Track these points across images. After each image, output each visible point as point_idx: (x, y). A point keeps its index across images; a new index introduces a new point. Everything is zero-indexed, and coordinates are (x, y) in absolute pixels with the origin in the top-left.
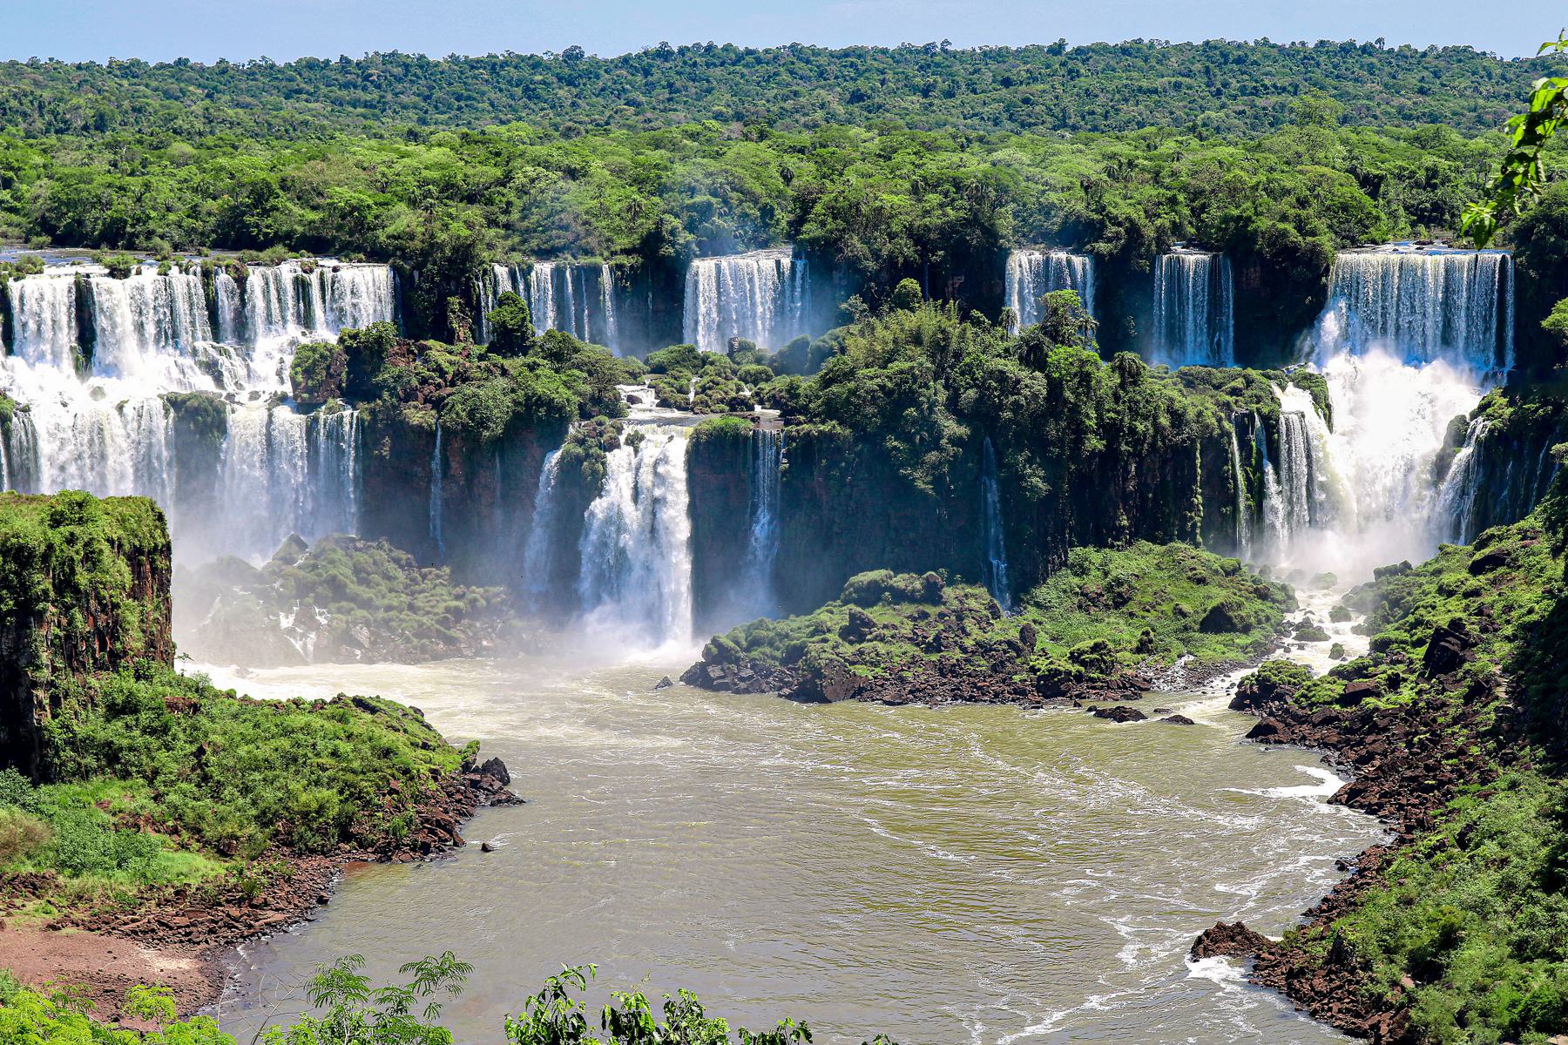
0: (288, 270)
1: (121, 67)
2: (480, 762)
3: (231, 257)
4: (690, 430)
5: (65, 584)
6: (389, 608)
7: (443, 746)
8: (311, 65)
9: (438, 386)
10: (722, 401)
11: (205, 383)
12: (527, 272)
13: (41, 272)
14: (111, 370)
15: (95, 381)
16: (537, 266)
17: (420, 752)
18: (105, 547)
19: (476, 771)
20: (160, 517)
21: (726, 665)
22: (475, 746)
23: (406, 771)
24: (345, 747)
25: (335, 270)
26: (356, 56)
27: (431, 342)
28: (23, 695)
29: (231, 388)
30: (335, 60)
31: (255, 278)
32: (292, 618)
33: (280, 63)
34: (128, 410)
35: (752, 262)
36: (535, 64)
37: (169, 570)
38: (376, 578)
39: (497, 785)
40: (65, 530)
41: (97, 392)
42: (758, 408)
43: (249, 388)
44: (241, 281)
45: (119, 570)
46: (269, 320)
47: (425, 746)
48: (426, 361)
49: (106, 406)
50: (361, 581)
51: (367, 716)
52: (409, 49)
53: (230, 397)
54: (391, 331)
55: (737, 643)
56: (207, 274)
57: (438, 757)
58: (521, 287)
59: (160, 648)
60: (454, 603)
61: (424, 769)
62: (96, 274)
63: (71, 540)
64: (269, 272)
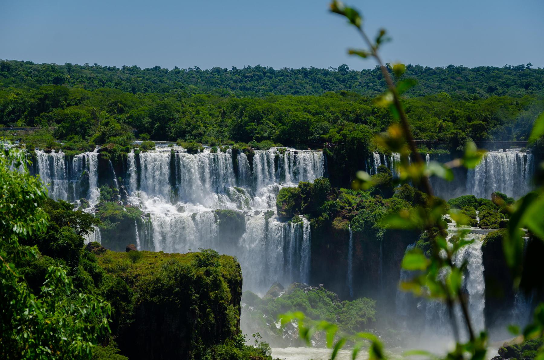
0: (272, 152)
1: (129, 69)
3: (246, 146)
5: (205, 296)
8: (218, 71)
9: (350, 211)
10: (495, 223)
11: (231, 206)
12: (388, 156)
13: (154, 149)
14: (188, 199)
15: (180, 203)
16: (393, 154)
20: (238, 266)
25: (296, 153)
26: (240, 68)
29: (245, 209)
30: (230, 69)
33: (203, 69)
34: (198, 217)
35: (504, 154)
36: (326, 73)
38: (320, 304)
40: (204, 269)
41: (181, 209)
43: (253, 210)
44: (250, 157)
46: (264, 177)
48: (341, 199)
49: (186, 215)
50: (313, 307)
52: (265, 64)
53: (245, 213)
54: (327, 182)
56: (235, 153)
58: (386, 164)
60: (360, 319)
62: (181, 151)
63: (208, 273)
64: (264, 152)
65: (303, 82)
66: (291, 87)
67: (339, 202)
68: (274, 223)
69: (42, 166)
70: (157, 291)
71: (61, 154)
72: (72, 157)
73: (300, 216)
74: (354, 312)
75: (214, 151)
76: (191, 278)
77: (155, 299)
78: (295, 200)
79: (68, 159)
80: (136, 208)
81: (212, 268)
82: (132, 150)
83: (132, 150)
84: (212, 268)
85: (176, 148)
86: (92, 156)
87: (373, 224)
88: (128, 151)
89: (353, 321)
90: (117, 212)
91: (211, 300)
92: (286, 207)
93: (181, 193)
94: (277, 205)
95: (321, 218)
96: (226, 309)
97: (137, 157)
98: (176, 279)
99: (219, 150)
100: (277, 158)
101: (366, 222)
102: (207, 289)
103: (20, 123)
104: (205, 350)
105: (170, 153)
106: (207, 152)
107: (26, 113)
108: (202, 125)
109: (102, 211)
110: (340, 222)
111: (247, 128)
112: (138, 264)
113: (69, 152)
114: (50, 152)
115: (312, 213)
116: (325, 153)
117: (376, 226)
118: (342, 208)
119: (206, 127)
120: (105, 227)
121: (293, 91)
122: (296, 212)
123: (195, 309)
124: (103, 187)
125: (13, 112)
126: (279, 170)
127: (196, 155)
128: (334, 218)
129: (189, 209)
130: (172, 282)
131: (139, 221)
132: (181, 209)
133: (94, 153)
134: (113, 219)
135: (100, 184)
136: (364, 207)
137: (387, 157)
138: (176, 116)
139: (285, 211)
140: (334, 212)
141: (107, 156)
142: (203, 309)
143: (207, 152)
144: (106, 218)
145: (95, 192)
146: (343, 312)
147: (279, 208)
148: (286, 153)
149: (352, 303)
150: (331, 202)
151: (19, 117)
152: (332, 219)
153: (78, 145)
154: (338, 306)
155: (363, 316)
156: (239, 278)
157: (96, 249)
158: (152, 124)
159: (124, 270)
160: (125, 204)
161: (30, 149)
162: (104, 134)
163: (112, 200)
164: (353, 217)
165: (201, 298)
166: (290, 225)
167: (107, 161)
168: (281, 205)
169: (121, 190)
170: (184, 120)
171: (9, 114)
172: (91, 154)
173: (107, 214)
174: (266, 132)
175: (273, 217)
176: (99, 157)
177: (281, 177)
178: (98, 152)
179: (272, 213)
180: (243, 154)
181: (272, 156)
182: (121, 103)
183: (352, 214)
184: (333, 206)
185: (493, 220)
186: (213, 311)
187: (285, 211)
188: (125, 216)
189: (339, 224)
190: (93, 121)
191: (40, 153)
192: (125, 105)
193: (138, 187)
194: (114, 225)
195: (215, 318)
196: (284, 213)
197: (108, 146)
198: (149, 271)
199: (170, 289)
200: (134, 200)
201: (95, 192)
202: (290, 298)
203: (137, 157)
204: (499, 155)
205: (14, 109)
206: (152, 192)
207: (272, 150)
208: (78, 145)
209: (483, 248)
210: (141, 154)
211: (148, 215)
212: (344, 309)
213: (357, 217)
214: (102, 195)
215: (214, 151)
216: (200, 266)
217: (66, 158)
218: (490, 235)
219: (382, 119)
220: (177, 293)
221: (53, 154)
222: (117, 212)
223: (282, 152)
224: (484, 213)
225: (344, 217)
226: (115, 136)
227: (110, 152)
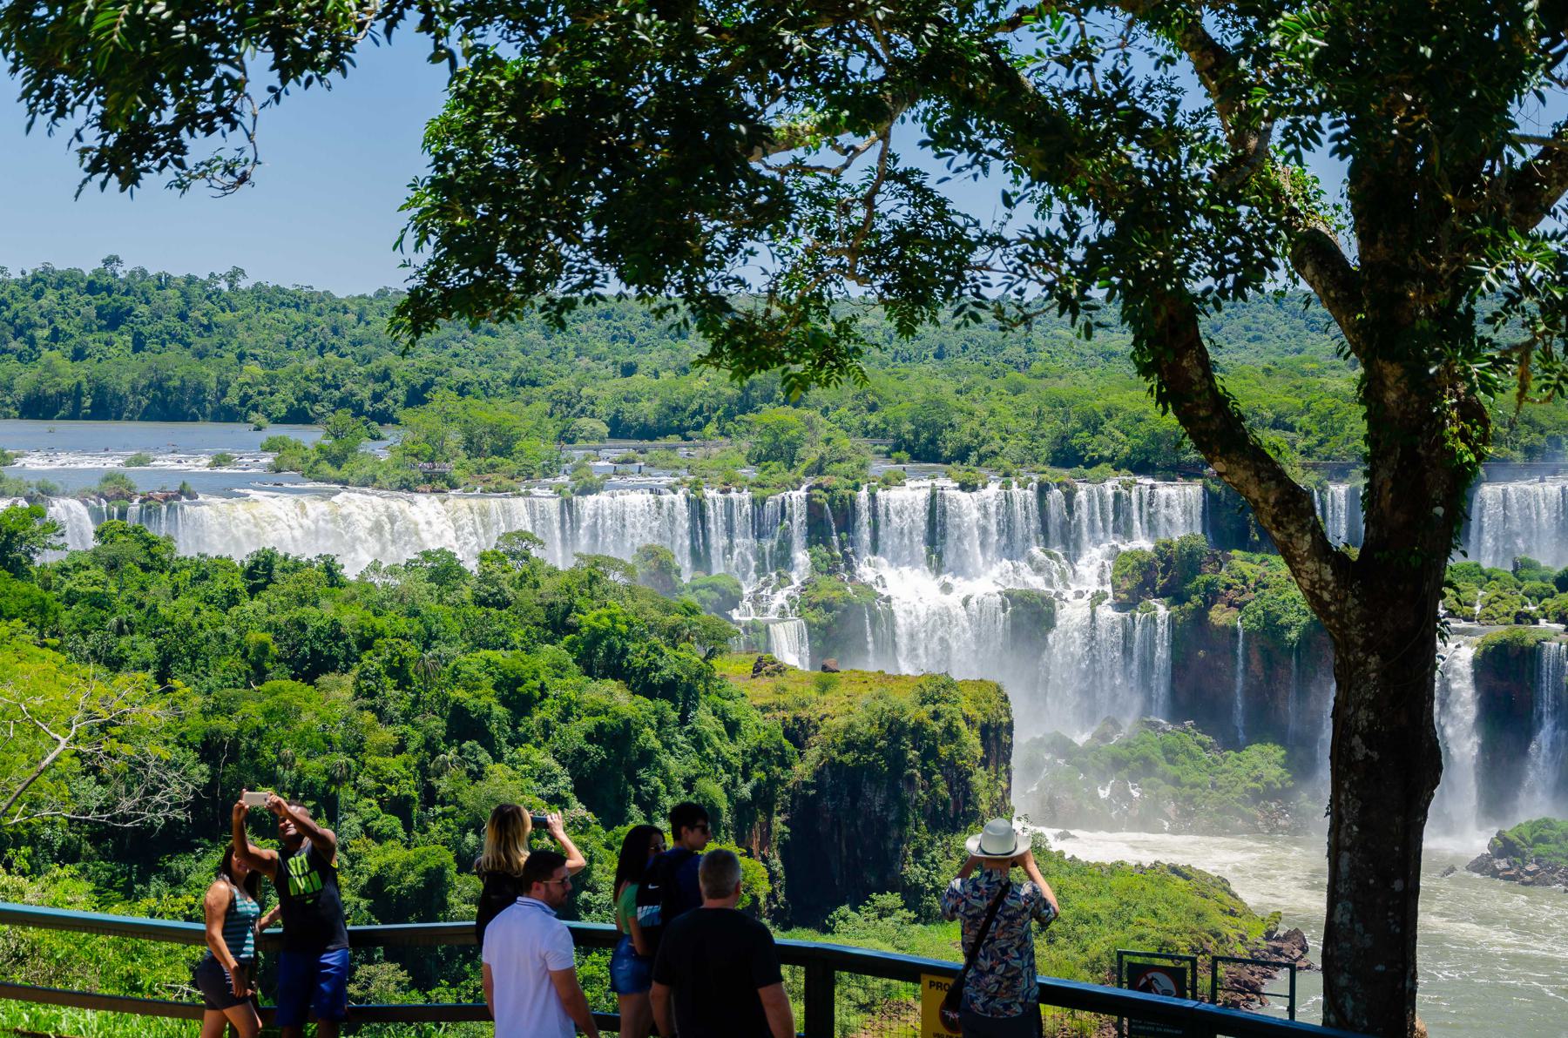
2: (1281, 933)
3: (1064, 474)
4: (1478, 640)
5: (930, 753)
6: (1194, 786)
7: (1247, 913)
9: (1243, 592)
10: (1507, 614)
11: (1037, 583)
14: (960, 571)
15: (948, 578)
16: (1332, 488)
17: (1228, 918)
18: (962, 724)
19: (1278, 939)
20: (1006, 699)
21: (1512, 859)
22: (1277, 917)
23: (1216, 935)
24: (1162, 909)
25: (1152, 487)
27: (1235, 552)
28: (891, 846)
29: (1060, 588)
31: (1081, 495)
32: (1108, 791)
34: (973, 601)
37: (1011, 745)
38: (1182, 757)
39: (1298, 953)
40: (930, 708)
41: (946, 588)
42: (1542, 622)
43: (1074, 587)
44: (1070, 496)
45: (972, 739)
46: (1092, 529)
47: (1232, 913)
48: (1229, 569)
49: (954, 600)
50: (1171, 762)
51: (1181, 881)
53: (1058, 595)
55: (1523, 839)
56: (1043, 489)
57: (1244, 923)
59: (1002, 808)
60: (1253, 785)
61: (1232, 933)
62: (948, 485)
63: (936, 716)
65: (1273, 318)
66: (1248, 329)
67: (1224, 576)
68: (1107, 612)
69: (715, 514)
70: (850, 745)
71: (746, 496)
72: (764, 501)
73: (1153, 602)
74: (1241, 772)
75: (1007, 486)
76: (904, 724)
77: (848, 758)
78: (1144, 573)
79: (758, 503)
80: (868, 586)
81: (942, 707)
82: (865, 487)
83: (865, 487)
84: (942, 707)
85: (940, 482)
86: (798, 496)
87: (1279, 617)
88: (857, 487)
89: (1240, 788)
90: (836, 594)
91: (941, 761)
92: (1127, 585)
93: (949, 557)
94: (1113, 582)
95: (1188, 605)
96: (970, 774)
97: (873, 497)
98: (881, 725)
99: (1015, 484)
100: (1117, 496)
101: (1267, 614)
102: (935, 740)
103: (710, 429)
104: (931, 843)
105: (928, 491)
106: (993, 489)
107: (720, 412)
108: (997, 437)
109: (810, 592)
110: (1223, 612)
111: (1074, 442)
112: (828, 696)
113: (759, 492)
114: (728, 491)
115: (1174, 594)
116: (1206, 488)
117: (1284, 620)
118: (1228, 587)
119: (1004, 440)
120: (815, 620)
121: (1250, 334)
122: (1145, 594)
123: (913, 775)
124: (815, 549)
125: (700, 411)
126: (1121, 518)
127: (974, 494)
128: (1213, 603)
129: (962, 587)
130: (875, 730)
131: (871, 608)
132: (946, 588)
133: (802, 492)
134: (828, 606)
135: (810, 543)
136: (1265, 587)
137: (1320, 492)
138: (957, 418)
139: (1126, 592)
140: (1212, 595)
141: (822, 498)
142: (927, 775)
143: (993, 489)
144: (816, 605)
145: (801, 557)
146: (1225, 771)
147: (1116, 588)
148: (1135, 489)
149: (1240, 755)
150: (1206, 578)
151: (708, 420)
152: (1208, 604)
153: (777, 478)
154: (1214, 761)
155: (1257, 779)
156: (1005, 720)
157: (770, 667)
158: (917, 434)
159: (804, 706)
160: (852, 579)
161: (695, 487)
162: (822, 458)
163: (831, 572)
164: (1245, 603)
165: (924, 758)
166: (1133, 617)
167: (821, 507)
168: (1119, 581)
169: (846, 555)
170: (967, 427)
171: (693, 415)
172: (795, 494)
173: (818, 598)
174: (1108, 447)
175: (1106, 602)
176: (809, 499)
177: (1123, 529)
178: (808, 490)
179: (1105, 596)
180: (1057, 491)
181: (1110, 492)
182: (874, 393)
183: (1244, 598)
184: (1208, 585)
185: (1506, 609)
186: (946, 777)
187: (1126, 592)
188: (848, 600)
189: (1220, 616)
190: (808, 435)
191: (711, 494)
192: (880, 397)
193: (875, 548)
194: (829, 616)
195: (950, 789)
196: (1124, 596)
197: (823, 480)
198: (844, 709)
199: (869, 744)
200: (865, 572)
201: (801, 557)
202: (1128, 745)
203: (873, 497)
204: (1530, 488)
205: (701, 406)
206: (896, 561)
207: (1109, 484)
208: (777, 478)
209: (1476, 663)
210: (880, 493)
211: (888, 600)
212: (1225, 766)
213: (1252, 604)
214: (814, 563)
215: (1007, 486)
216: (924, 703)
217: (753, 501)
218: (1489, 640)
219: (1320, 422)
220: (881, 750)
221: (733, 495)
222: (836, 594)
223: (1128, 487)
224: (1491, 595)
225: (1231, 604)
226: (839, 461)
227: (827, 491)
